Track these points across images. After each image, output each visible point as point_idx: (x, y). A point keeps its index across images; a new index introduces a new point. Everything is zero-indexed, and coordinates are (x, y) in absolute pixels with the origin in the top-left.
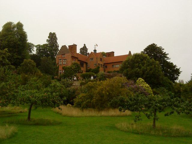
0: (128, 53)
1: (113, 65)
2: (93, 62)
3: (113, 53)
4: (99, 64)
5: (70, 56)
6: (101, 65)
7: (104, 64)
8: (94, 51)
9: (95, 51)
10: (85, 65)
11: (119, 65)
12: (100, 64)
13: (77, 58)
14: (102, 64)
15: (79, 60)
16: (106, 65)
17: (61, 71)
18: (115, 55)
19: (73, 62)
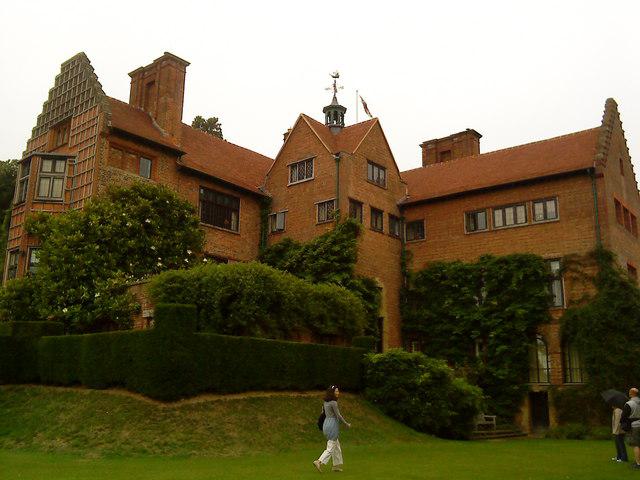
0: (594, 120)
1: (472, 217)
2: (310, 185)
3: (472, 137)
4: (356, 204)
5: (96, 131)
6: (376, 212)
7: (403, 207)
8: (328, 115)
9: (335, 111)
10: (247, 215)
11: (521, 210)
12: (366, 210)
13: (176, 154)
14: (388, 208)
15: (186, 172)
16: (413, 216)
17: (15, 252)
18: (486, 147)
19: (129, 177)
